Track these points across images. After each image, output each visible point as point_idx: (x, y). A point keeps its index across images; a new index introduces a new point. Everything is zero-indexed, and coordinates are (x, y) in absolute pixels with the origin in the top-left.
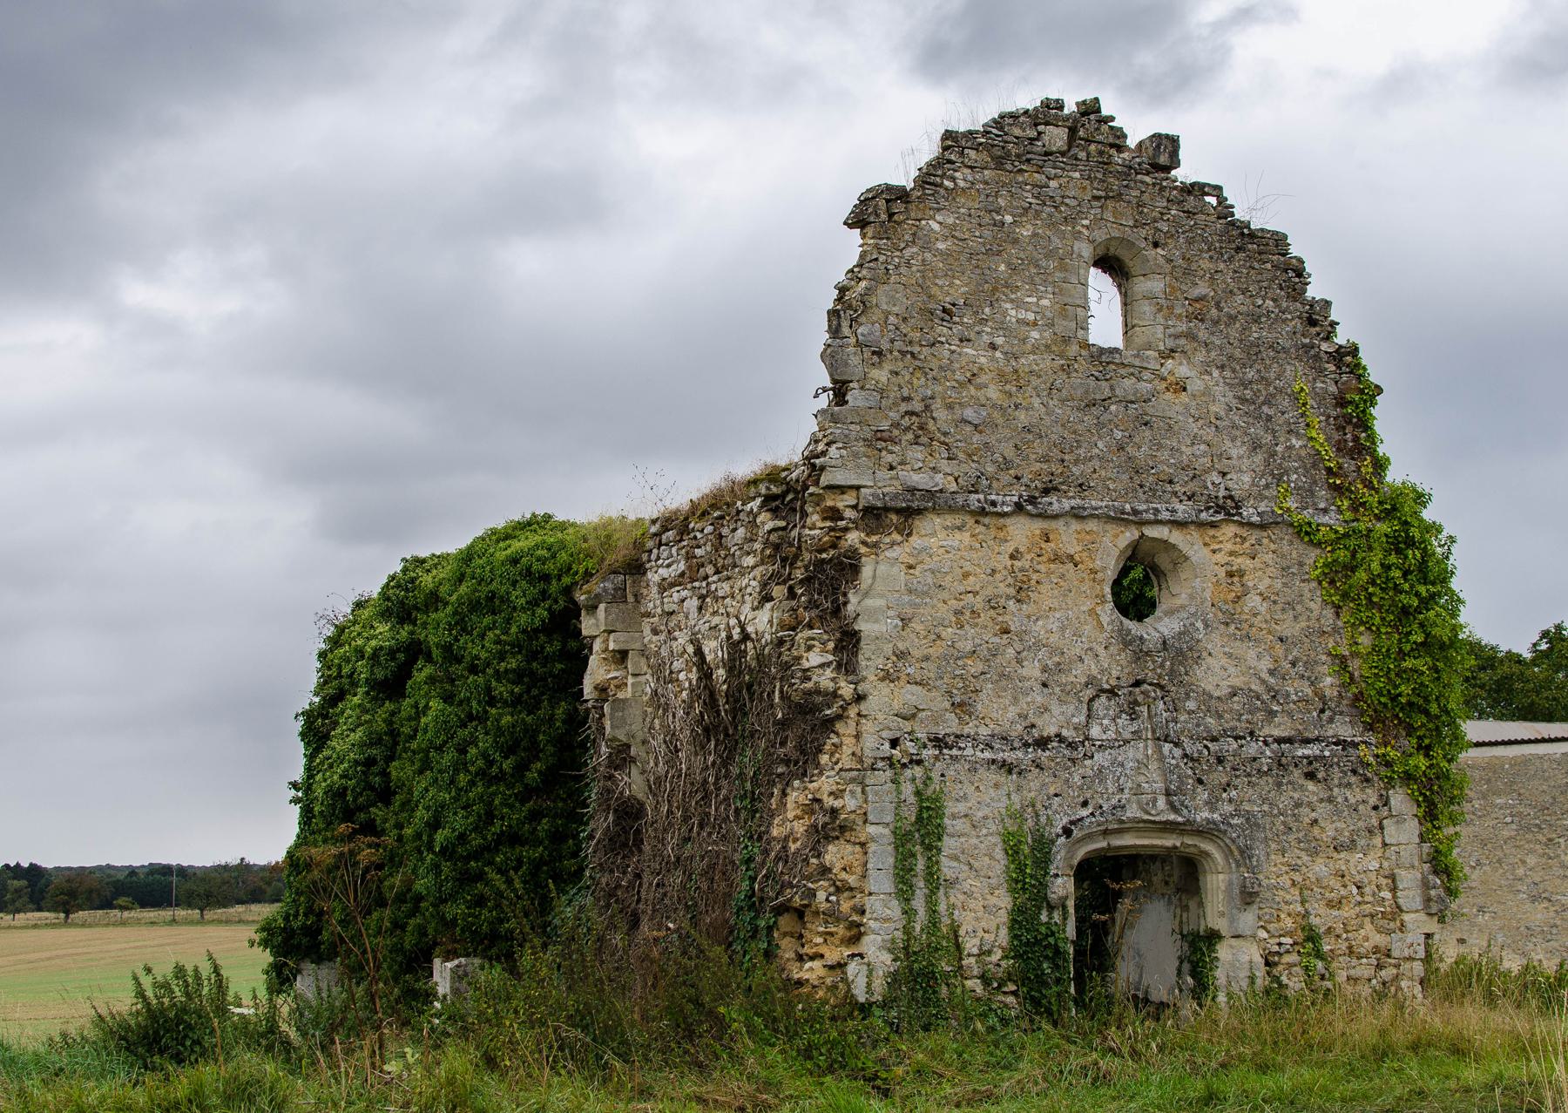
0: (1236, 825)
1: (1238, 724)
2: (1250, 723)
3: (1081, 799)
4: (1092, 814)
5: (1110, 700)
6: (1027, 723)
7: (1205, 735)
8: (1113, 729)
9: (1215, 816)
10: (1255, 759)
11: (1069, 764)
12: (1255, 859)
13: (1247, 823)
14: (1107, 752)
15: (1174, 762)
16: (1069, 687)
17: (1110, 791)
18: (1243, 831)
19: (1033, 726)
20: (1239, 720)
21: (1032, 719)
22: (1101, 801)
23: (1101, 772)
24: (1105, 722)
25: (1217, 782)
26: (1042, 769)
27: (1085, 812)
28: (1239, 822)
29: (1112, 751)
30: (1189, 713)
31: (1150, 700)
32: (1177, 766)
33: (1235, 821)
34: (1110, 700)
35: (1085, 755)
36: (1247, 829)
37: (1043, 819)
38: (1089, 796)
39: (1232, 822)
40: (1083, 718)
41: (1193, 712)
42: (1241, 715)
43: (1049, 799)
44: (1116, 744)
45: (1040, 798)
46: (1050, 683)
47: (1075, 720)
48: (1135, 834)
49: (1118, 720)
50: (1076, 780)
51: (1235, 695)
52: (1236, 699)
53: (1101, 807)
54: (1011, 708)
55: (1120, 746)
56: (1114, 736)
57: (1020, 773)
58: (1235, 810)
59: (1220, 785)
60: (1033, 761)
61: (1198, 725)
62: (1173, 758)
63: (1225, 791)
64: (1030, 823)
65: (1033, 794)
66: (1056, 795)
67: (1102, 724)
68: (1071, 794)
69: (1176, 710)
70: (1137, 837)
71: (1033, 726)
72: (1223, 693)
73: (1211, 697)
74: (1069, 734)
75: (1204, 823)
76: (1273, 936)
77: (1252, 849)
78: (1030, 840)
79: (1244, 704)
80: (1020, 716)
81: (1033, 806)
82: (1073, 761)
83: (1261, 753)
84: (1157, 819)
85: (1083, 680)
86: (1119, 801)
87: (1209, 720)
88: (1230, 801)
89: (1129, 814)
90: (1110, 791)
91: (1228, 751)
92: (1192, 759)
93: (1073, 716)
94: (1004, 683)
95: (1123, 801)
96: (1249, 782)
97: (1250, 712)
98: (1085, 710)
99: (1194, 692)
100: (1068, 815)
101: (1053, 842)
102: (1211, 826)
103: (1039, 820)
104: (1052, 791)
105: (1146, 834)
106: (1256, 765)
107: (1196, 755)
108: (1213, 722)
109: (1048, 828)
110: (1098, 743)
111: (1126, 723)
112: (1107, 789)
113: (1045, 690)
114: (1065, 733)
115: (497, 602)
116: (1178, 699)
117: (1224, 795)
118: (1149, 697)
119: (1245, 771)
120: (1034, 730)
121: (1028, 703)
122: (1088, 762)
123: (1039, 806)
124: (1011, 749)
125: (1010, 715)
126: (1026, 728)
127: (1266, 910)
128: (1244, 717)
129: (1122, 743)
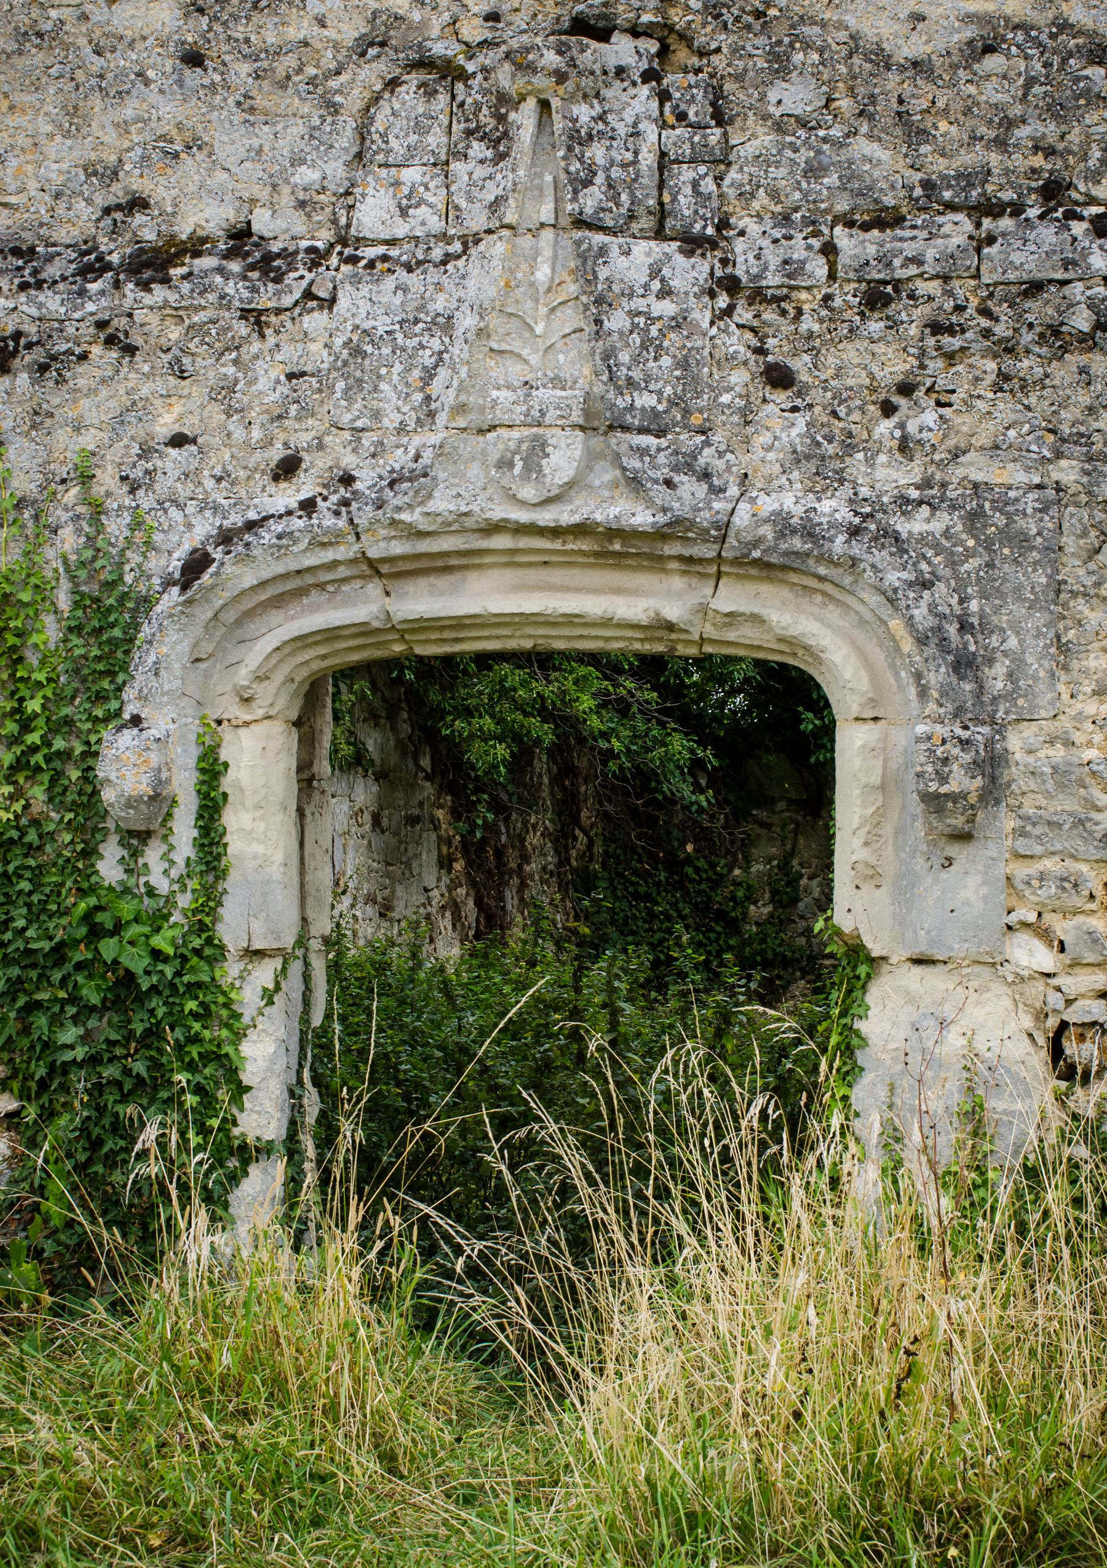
0: (922, 538)
1: (994, 159)
2: (1050, 152)
3: (277, 453)
4: (308, 506)
5: (431, 94)
6: (117, 193)
7: (842, 206)
8: (439, 197)
9: (826, 506)
10: (1035, 288)
11: (242, 329)
12: (1000, 669)
13: (971, 530)
14: (390, 282)
15: (666, 308)
16: (290, 61)
17: (390, 420)
18: (953, 563)
19: (138, 203)
20: (1001, 144)
21: (135, 182)
22: (349, 461)
23: (357, 352)
24: (411, 175)
25: (857, 379)
26: (130, 350)
27: (286, 497)
28: (937, 526)
29: (413, 280)
30: (779, 128)
31: (541, 82)
32: (679, 322)
33: (917, 524)
34: (431, 94)
35: (308, 295)
36: (969, 554)
37: (116, 527)
38: (303, 439)
39: (903, 527)
40: (336, 169)
41: (803, 123)
42: (1010, 124)
43: (146, 452)
44: (437, 254)
45: (113, 455)
46: (218, 48)
47: (307, 175)
48: (511, 576)
49: (456, 167)
50: (263, 384)
51: (989, 49)
52: (993, 63)
53: (347, 480)
54: (56, 147)
55: (447, 259)
56: (436, 224)
57: (43, 368)
58: (926, 484)
59: (873, 390)
60: (101, 325)
61: (813, 171)
62: (665, 293)
63: (888, 409)
64: (69, 540)
65: (89, 440)
66: (179, 441)
67: (397, 184)
68: (239, 434)
69: (719, 118)
70: (520, 588)
71: (138, 203)
72: (940, 45)
73: (882, 60)
74: (279, 224)
75: (767, 532)
76: (1076, 964)
77: (986, 628)
78: (64, 601)
79: (1030, 82)
80: (90, 171)
81: (86, 479)
82: (256, 318)
83: (1067, 264)
84: (546, 517)
85: (350, 30)
86: (417, 458)
87: (862, 147)
88: (905, 447)
89: (442, 503)
90: (390, 420)
91: (917, 260)
92: (758, 296)
93: (297, 161)
94: (37, 58)
95: (427, 456)
96: (1004, 376)
97: (1056, 111)
98: (346, 140)
99: (807, 46)
100: (216, 508)
101: (146, 602)
102: (797, 543)
103: (100, 528)
104: (165, 424)
105: (556, 576)
106: (1038, 310)
107: (772, 279)
108: (884, 155)
109: (134, 558)
110: (371, 252)
111: (481, 172)
112: (377, 415)
113: (193, 77)
114: (263, 221)
115: (591, 199)
116: (739, 77)
117: (885, 427)
118: (531, 69)
119: (987, 333)
120: (139, 219)
121: (123, 127)
122: (316, 321)
123: (107, 479)
124: (24, 287)
125: (54, 174)
126: (107, 211)
127: (1048, 864)
128: (1022, 133)
129: (457, 247)
